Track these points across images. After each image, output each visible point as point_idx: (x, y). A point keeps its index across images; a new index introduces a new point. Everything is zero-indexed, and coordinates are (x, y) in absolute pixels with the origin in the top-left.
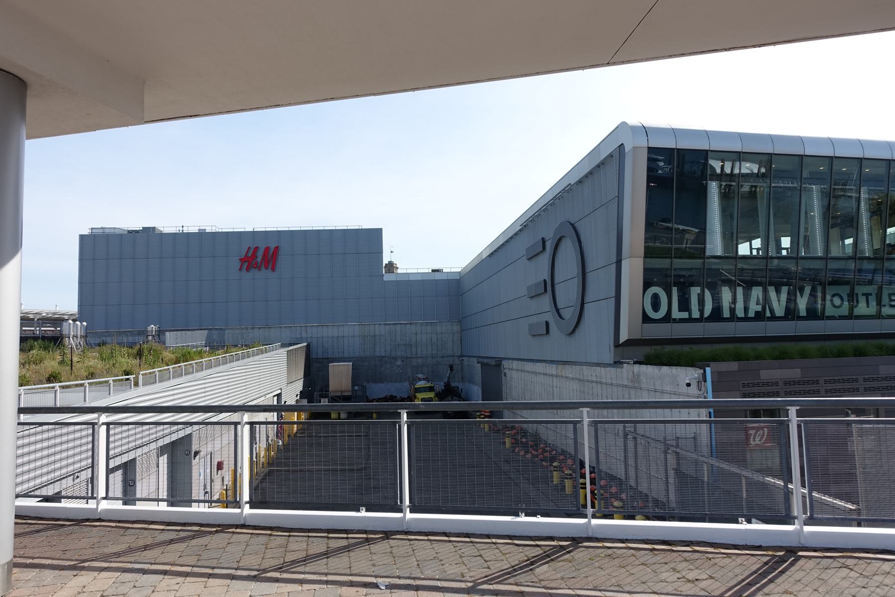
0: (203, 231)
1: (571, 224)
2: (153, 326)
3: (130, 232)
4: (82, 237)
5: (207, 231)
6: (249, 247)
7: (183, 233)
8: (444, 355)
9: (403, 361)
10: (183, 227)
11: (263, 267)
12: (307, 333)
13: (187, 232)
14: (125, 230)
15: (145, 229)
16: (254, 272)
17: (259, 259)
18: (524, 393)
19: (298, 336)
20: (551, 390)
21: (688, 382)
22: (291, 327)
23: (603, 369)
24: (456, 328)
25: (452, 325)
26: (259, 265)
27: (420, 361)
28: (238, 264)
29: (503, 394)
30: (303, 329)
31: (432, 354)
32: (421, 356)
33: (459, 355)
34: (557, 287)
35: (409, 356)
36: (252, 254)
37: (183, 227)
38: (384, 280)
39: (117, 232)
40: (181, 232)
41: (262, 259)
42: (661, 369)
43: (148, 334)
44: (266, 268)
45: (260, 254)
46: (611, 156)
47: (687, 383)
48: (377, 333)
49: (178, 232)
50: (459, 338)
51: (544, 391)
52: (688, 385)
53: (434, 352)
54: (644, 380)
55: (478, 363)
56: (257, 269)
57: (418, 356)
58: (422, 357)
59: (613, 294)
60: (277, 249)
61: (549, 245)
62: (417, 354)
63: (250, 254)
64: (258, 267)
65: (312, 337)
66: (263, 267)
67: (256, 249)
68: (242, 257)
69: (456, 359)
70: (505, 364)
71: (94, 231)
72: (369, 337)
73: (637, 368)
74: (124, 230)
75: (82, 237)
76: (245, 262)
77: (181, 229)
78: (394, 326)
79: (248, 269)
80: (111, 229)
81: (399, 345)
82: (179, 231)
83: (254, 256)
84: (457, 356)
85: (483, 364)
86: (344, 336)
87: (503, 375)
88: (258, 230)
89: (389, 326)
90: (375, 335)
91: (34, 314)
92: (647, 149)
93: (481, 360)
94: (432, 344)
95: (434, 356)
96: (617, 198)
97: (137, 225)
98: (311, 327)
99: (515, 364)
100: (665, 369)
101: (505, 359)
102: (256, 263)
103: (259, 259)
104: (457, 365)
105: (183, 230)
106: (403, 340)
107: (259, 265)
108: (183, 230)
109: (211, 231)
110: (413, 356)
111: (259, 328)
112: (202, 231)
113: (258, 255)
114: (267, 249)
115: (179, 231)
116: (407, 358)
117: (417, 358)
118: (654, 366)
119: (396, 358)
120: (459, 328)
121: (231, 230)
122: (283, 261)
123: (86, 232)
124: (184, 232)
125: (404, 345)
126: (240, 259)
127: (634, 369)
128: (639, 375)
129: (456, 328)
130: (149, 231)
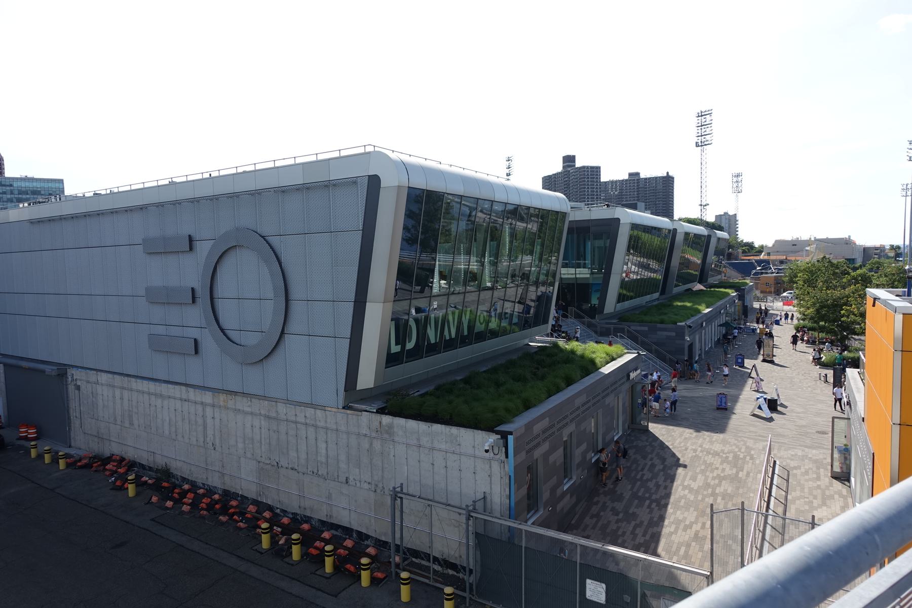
1: (263, 237)
18: (130, 417)
20: (200, 421)
21: (487, 448)
23: (319, 412)
29: (71, 411)
34: (220, 305)
42: (431, 426)
46: (353, 182)
47: (485, 450)
51: (183, 420)
52: (487, 451)
54: (400, 433)
59: (348, 333)
61: (203, 248)
70: (70, 372)
73: (386, 419)
87: (71, 388)
92: (407, 189)
96: (361, 232)
99: (104, 378)
100: (437, 427)
101: (73, 366)
118: (419, 422)
127: (381, 419)
128: (391, 426)
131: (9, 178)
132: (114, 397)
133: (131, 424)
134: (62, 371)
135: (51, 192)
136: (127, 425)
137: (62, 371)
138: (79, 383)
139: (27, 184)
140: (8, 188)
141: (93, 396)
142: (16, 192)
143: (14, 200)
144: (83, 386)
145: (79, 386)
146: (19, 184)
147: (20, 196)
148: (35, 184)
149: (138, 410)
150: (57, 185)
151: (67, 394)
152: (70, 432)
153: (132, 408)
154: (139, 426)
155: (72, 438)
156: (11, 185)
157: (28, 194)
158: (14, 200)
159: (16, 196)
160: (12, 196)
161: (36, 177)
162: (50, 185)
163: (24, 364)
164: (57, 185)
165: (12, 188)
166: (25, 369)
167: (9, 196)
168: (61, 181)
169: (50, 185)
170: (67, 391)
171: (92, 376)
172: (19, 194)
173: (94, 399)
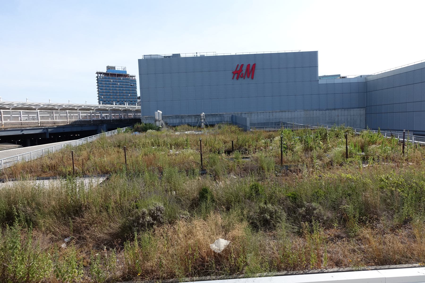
0: (203, 56)
2: (203, 113)
4: (140, 61)
5: (205, 56)
6: (238, 65)
7: (197, 57)
10: (197, 53)
11: (246, 76)
12: (273, 116)
13: (206, 56)
15: (174, 55)
16: (240, 79)
17: (244, 72)
24: (363, 111)
25: (360, 110)
26: (244, 75)
28: (232, 75)
30: (271, 113)
36: (240, 69)
37: (197, 53)
39: (159, 57)
40: (196, 56)
43: (202, 118)
44: (248, 77)
45: (244, 69)
49: (194, 56)
50: (364, 118)
56: (243, 78)
60: (254, 65)
63: (238, 69)
64: (243, 77)
65: (276, 119)
66: (246, 76)
67: (242, 65)
68: (233, 71)
71: (146, 57)
74: (162, 56)
75: (140, 61)
78: (325, 112)
79: (237, 78)
80: (155, 56)
82: (195, 56)
83: (241, 70)
88: (218, 55)
89: (322, 112)
91: (58, 106)
93: (415, 133)
94: (348, 122)
97: (169, 53)
98: (275, 112)
102: (242, 74)
103: (244, 72)
105: (197, 55)
107: (244, 75)
108: (197, 55)
109: (213, 55)
111: (245, 113)
112: (201, 56)
113: (243, 69)
114: (249, 65)
115: (195, 56)
121: (242, 54)
122: (257, 72)
123: (141, 58)
124: (198, 56)
126: (233, 72)
129: (363, 111)
130: (176, 56)
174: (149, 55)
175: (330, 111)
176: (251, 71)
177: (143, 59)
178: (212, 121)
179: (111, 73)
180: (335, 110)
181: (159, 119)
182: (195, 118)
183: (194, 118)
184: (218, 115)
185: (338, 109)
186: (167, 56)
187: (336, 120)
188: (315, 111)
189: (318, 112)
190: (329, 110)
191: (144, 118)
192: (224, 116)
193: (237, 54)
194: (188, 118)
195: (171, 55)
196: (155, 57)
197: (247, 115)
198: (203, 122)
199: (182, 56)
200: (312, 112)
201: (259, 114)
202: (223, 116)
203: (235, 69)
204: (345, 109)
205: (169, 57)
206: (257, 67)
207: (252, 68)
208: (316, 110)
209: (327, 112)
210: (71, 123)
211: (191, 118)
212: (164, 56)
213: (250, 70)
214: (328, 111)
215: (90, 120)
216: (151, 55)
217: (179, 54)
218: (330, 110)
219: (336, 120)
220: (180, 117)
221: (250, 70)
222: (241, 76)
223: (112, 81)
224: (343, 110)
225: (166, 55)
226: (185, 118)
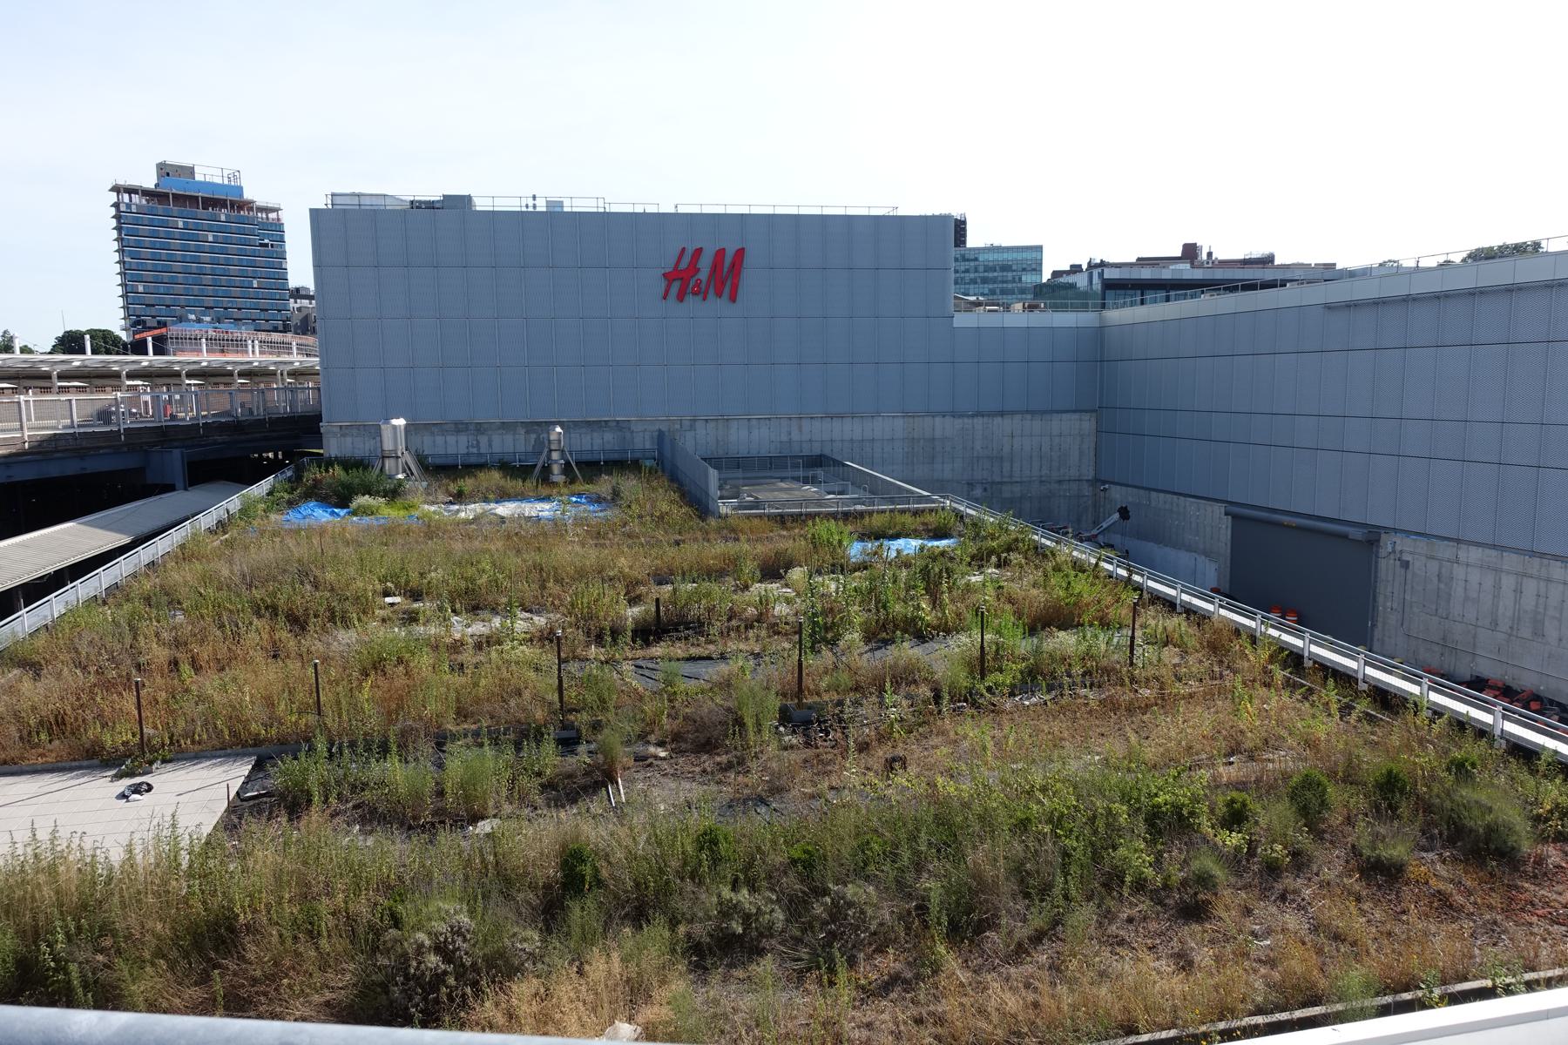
0: (558, 209)
3: (414, 204)
4: (315, 214)
6: (684, 249)
8: (1062, 478)
9: (985, 490)
10: (534, 197)
11: (712, 290)
12: (801, 431)
14: (405, 201)
19: (784, 438)
22: (769, 419)
24: (1087, 424)
25: (1081, 420)
27: (1017, 489)
31: (1041, 476)
32: (1019, 480)
33: (1090, 478)
35: (998, 479)
37: (534, 197)
38: (955, 326)
41: (710, 275)
44: (719, 294)
45: (705, 264)
48: (938, 434)
49: (524, 209)
50: (1093, 445)
53: (1043, 473)
55: (1226, 514)
57: (1015, 479)
58: (1021, 482)
60: (740, 253)
62: (1011, 476)
63: (684, 264)
66: (712, 290)
67: (698, 252)
68: (667, 270)
69: (1085, 486)
71: (338, 200)
72: (922, 441)
76: (673, 280)
77: (531, 203)
78: (970, 421)
79: (681, 297)
81: (978, 457)
82: (527, 206)
83: (693, 268)
84: (1088, 481)
85: (1236, 518)
86: (873, 439)
89: (960, 421)
90: (934, 439)
95: (1043, 479)
97: (431, 191)
99: (1475, 554)
101: (1396, 531)
103: (703, 275)
104: (1085, 499)
105: (535, 206)
106: (987, 447)
108: (535, 206)
110: (1005, 480)
111: (706, 420)
113: (699, 265)
114: (721, 253)
116: (993, 483)
117: (1012, 483)
119: (972, 484)
120: (1094, 426)
122: (750, 279)
125: (988, 457)
129: (1087, 424)
130: (458, 204)
131: (974, 249)
132: (1497, 586)
133: (1538, 633)
134: (1372, 538)
135: (1024, 266)
136: (1526, 632)
137: (1372, 538)
138: (1406, 557)
139: (996, 256)
140: (972, 264)
141: (1439, 580)
142: (981, 269)
143: (979, 281)
144: (1417, 565)
145: (1408, 562)
146: (986, 256)
147: (986, 274)
148: (1005, 255)
149: (1561, 614)
150: (1034, 255)
151: (1376, 572)
152: (1372, 630)
153: (1545, 609)
154: (1560, 640)
155: (1375, 640)
156: (976, 259)
157: (995, 271)
158: (979, 281)
159: (981, 275)
160: (976, 274)
161: (1004, 244)
162: (1025, 255)
163: (1286, 519)
164: (1034, 255)
165: (977, 263)
166: (1288, 527)
167: (972, 275)
168: (1039, 249)
169: (1025, 255)
170: (1376, 567)
171: (1445, 550)
172: (985, 271)
173: (1442, 586)
174: (353, 195)
175: (986, 419)
176: (729, 272)
177: (330, 207)
178: (590, 448)
179: (174, 191)
180: (1002, 416)
181: (395, 451)
182: (527, 432)
183: (523, 432)
184: (610, 424)
185: (1013, 413)
186: (420, 202)
187: (1007, 449)
188: (938, 420)
189: (948, 420)
190: (983, 416)
191: (335, 429)
192: (633, 428)
193: (681, 210)
194: (500, 432)
195: (438, 198)
196: (374, 201)
197: (712, 425)
198: (556, 462)
199: (481, 204)
200: (928, 420)
201: (754, 422)
202: (629, 429)
203: (673, 266)
204: (1033, 413)
205: (430, 205)
206: (748, 260)
207: (733, 265)
208: (944, 416)
209: (979, 421)
210: (36, 444)
211: (514, 434)
212: (412, 202)
213: (725, 270)
214: (980, 419)
215: (116, 429)
216: (359, 195)
217: (469, 198)
218: (989, 416)
219: (1007, 449)
220: (471, 427)
221: (725, 270)
222: (693, 289)
223: (181, 225)
224: (1029, 417)
225: (417, 198)
226: (490, 432)
